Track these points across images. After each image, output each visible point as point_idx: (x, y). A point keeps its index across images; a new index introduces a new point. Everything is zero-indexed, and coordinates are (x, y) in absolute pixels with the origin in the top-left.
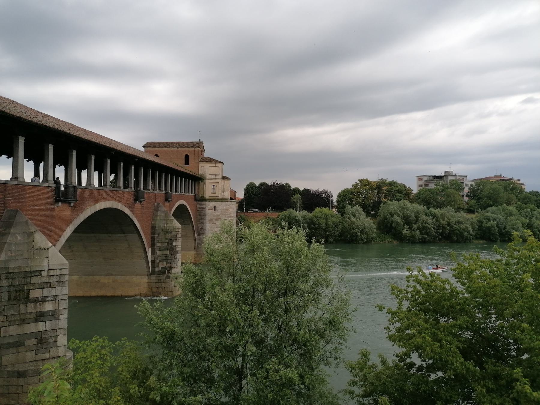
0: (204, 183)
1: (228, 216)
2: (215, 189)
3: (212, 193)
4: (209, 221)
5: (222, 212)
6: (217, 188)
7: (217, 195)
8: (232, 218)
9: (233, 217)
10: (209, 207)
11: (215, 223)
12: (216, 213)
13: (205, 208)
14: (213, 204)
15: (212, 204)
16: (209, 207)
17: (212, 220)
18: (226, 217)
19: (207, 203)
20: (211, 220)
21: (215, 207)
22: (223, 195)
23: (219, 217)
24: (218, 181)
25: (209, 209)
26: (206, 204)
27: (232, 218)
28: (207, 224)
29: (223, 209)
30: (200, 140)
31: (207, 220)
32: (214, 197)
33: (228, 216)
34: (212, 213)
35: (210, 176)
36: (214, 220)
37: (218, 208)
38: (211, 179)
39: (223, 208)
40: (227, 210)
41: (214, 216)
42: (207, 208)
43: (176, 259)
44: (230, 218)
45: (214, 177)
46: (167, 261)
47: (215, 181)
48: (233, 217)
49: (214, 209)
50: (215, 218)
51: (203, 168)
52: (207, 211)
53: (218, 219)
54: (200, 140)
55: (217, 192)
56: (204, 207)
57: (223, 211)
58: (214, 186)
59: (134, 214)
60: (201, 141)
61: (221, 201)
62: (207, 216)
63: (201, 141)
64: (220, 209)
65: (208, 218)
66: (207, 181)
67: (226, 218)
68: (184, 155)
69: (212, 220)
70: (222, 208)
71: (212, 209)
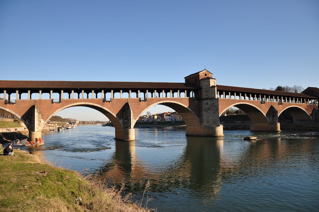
0: (202, 91)
3: (206, 96)
4: (204, 110)
5: (211, 105)
7: (208, 96)
12: (208, 106)
15: (205, 102)
17: (206, 110)
19: (203, 101)
20: (205, 110)
28: (204, 112)
29: (212, 104)
31: (203, 110)
35: (204, 87)
38: (205, 88)
39: (211, 103)
40: (214, 104)
41: (207, 108)
42: (203, 104)
44: (215, 108)
45: (206, 87)
50: (208, 108)
53: (209, 109)
59: (103, 106)
62: (203, 108)
65: (204, 109)
66: (203, 90)
67: (213, 108)
69: (206, 110)
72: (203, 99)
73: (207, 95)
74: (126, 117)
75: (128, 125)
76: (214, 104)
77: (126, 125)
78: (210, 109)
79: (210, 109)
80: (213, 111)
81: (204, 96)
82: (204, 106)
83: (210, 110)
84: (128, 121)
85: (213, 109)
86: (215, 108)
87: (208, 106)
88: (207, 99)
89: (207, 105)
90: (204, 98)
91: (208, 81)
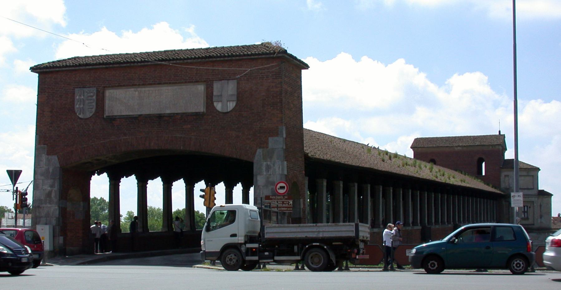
2: (527, 212)
22: (541, 222)
24: (533, 199)
30: (500, 132)
51: (507, 178)
54: (500, 132)
55: (530, 217)
60: (501, 134)
63: (501, 134)
68: (476, 158)
91: (533, 176)
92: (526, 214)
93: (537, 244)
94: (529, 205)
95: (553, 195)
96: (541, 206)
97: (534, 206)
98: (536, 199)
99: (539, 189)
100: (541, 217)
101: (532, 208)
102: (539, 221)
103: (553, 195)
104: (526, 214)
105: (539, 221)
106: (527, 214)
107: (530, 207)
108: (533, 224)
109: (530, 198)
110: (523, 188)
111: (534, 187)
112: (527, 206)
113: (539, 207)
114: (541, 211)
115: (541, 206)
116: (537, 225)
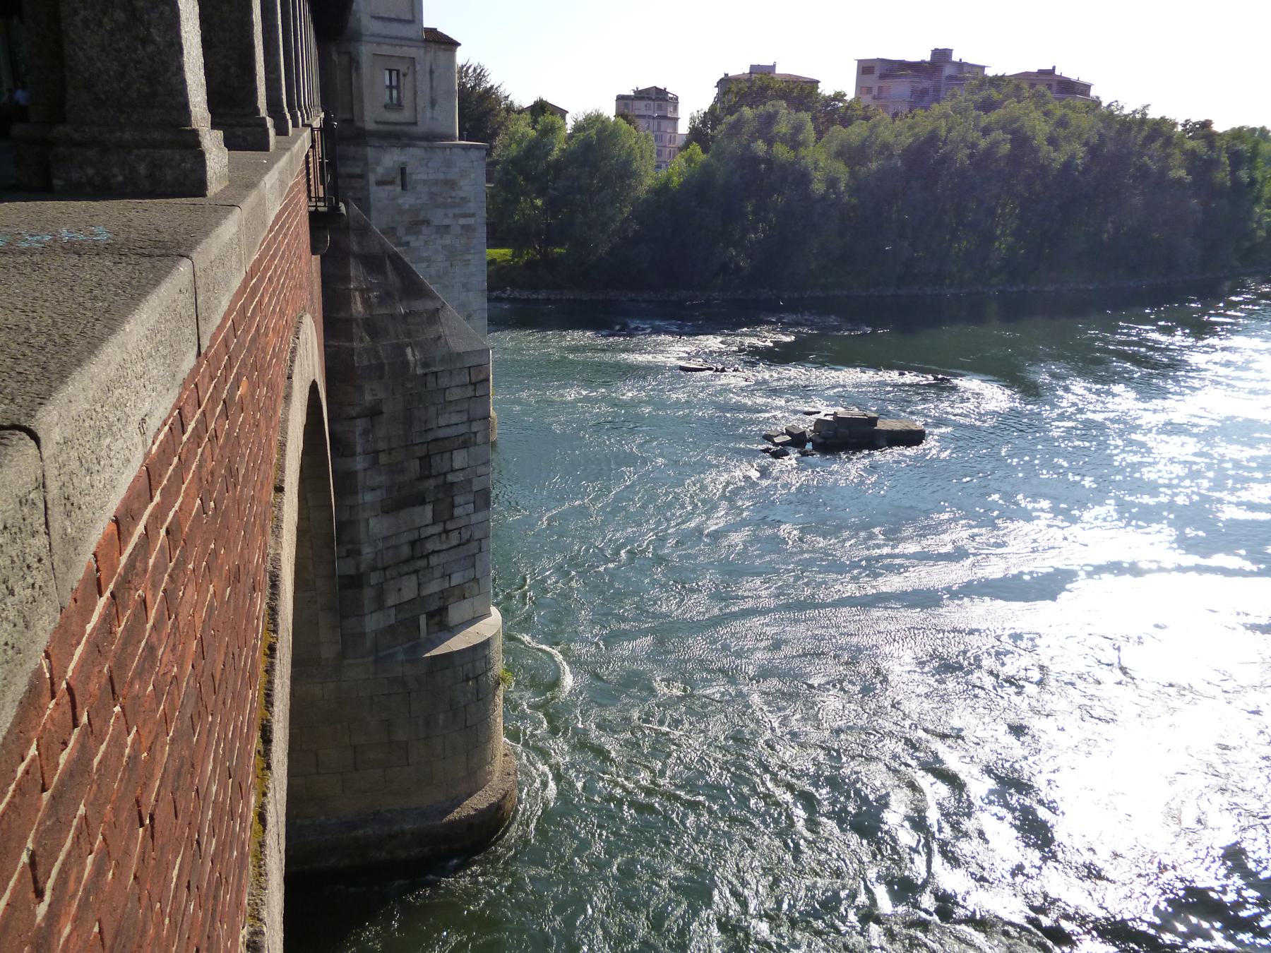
1: (457, 211)
2: (398, 88)
3: (386, 106)
5: (432, 196)
6: (407, 84)
7: (405, 115)
8: (471, 221)
9: (473, 215)
10: (380, 170)
11: (407, 244)
12: (407, 201)
13: (361, 176)
14: (396, 158)
15: (390, 159)
16: (380, 170)
18: (446, 215)
19: (370, 152)
21: (403, 170)
22: (432, 118)
23: (421, 218)
25: (379, 183)
26: (365, 160)
27: (471, 221)
29: (436, 182)
32: (398, 128)
33: (457, 211)
34: (393, 199)
35: (376, 27)
36: (401, 231)
37: (418, 174)
40: (452, 184)
42: (372, 178)
43: (468, 541)
44: (462, 221)
46: (422, 563)
47: (398, 51)
48: (473, 215)
49: (398, 181)
52: (373, 188)
55: (406, 102)
56: (358, 171)
57: (434, 189)
58: (394, 73)
61: (425, 144)
64: (424, 182)
67: (447, 222)
70: (431, 177)
71: (392, 183)
72: (361, 137)
73: (398, 106)
74: (414, 466)
75: (433, 587)
76: (452, 184)
77: (409, 589)
78: (427, 222)
79: (427, 222)
80: (448, 240)
81: (372, 113)
82: (379, 195)
83: (425, 230)
84: (445, 514)
85: (448, 226)
86: (462, 221)
87: (407, 201)
88: (397, 137)
89: (404, 187)
90: (370, 125)
92: (395, 93)
93: (424, 177)
94: (403, 69)
95: (459, 44)
96: (431, 72)
97: (415, 72)
98: (422, 51)
99: (428, 23)
100: (433, 103)
101: (409, 78)
102: (428, 113)
103: (459, 44)
104: (395, 93)
105: (428, 113)
106: (399, 94)
107: (405, 75)
108: (415, 124)
109: (405, 48)
110: (386, 16)
111: (414, 16)
112: (398, 72)
113: (428, 75)
114: (432, 87)
115: (431, 72)
116: (421, 128)
